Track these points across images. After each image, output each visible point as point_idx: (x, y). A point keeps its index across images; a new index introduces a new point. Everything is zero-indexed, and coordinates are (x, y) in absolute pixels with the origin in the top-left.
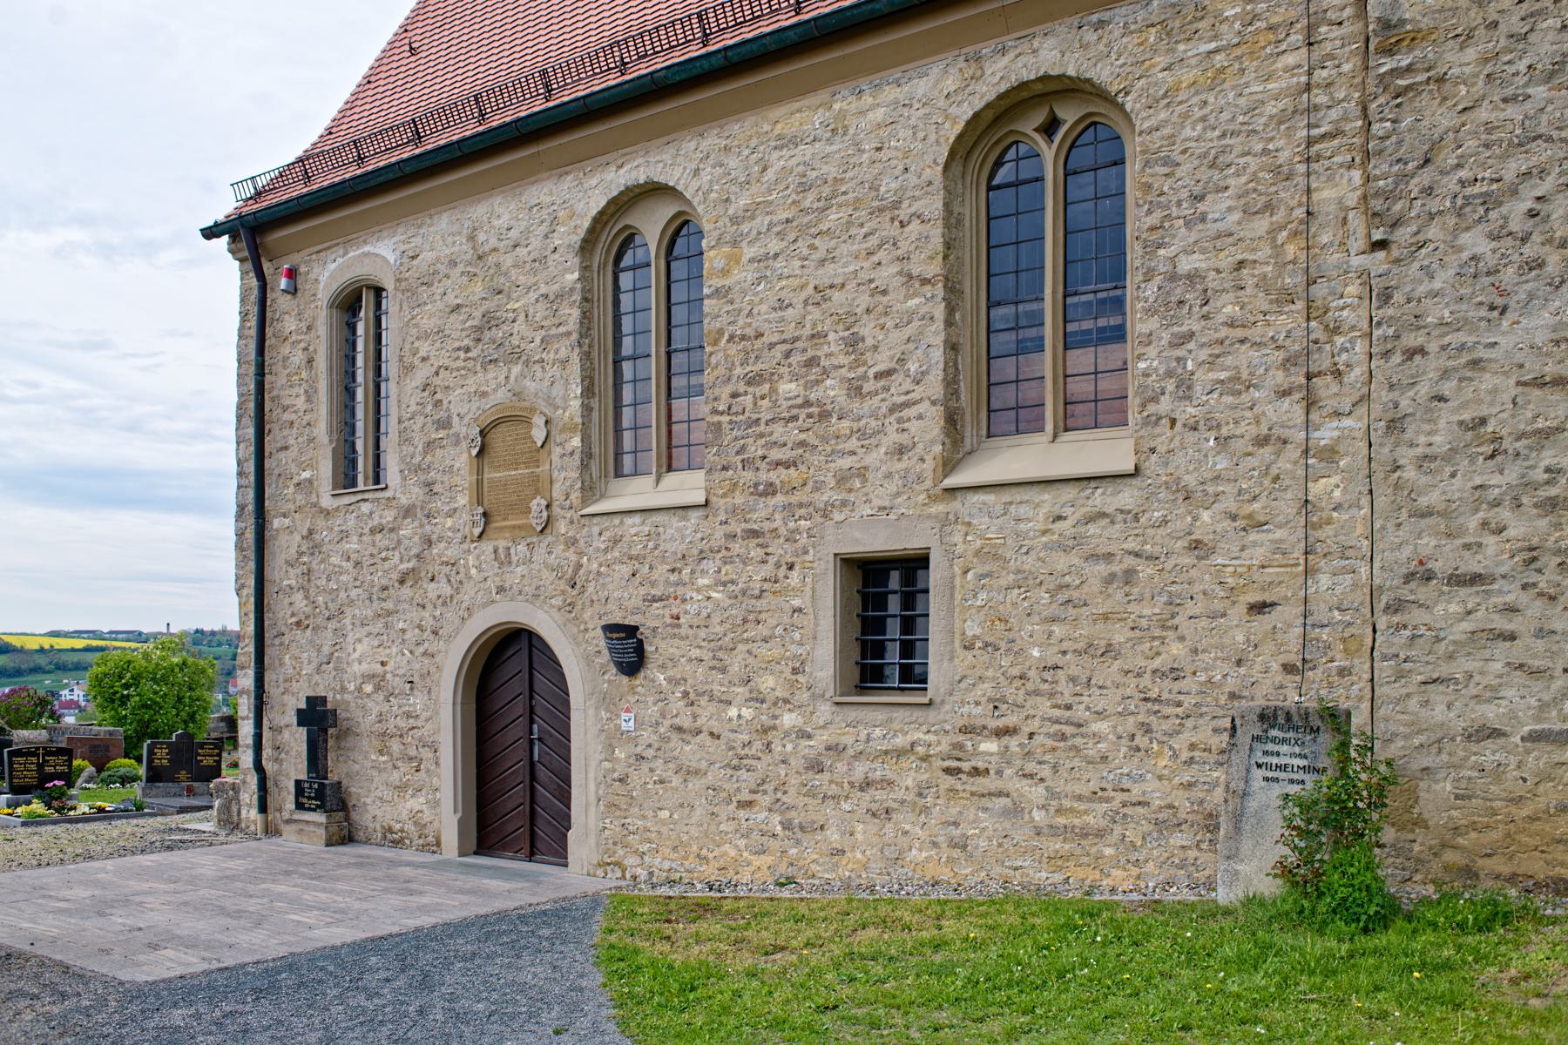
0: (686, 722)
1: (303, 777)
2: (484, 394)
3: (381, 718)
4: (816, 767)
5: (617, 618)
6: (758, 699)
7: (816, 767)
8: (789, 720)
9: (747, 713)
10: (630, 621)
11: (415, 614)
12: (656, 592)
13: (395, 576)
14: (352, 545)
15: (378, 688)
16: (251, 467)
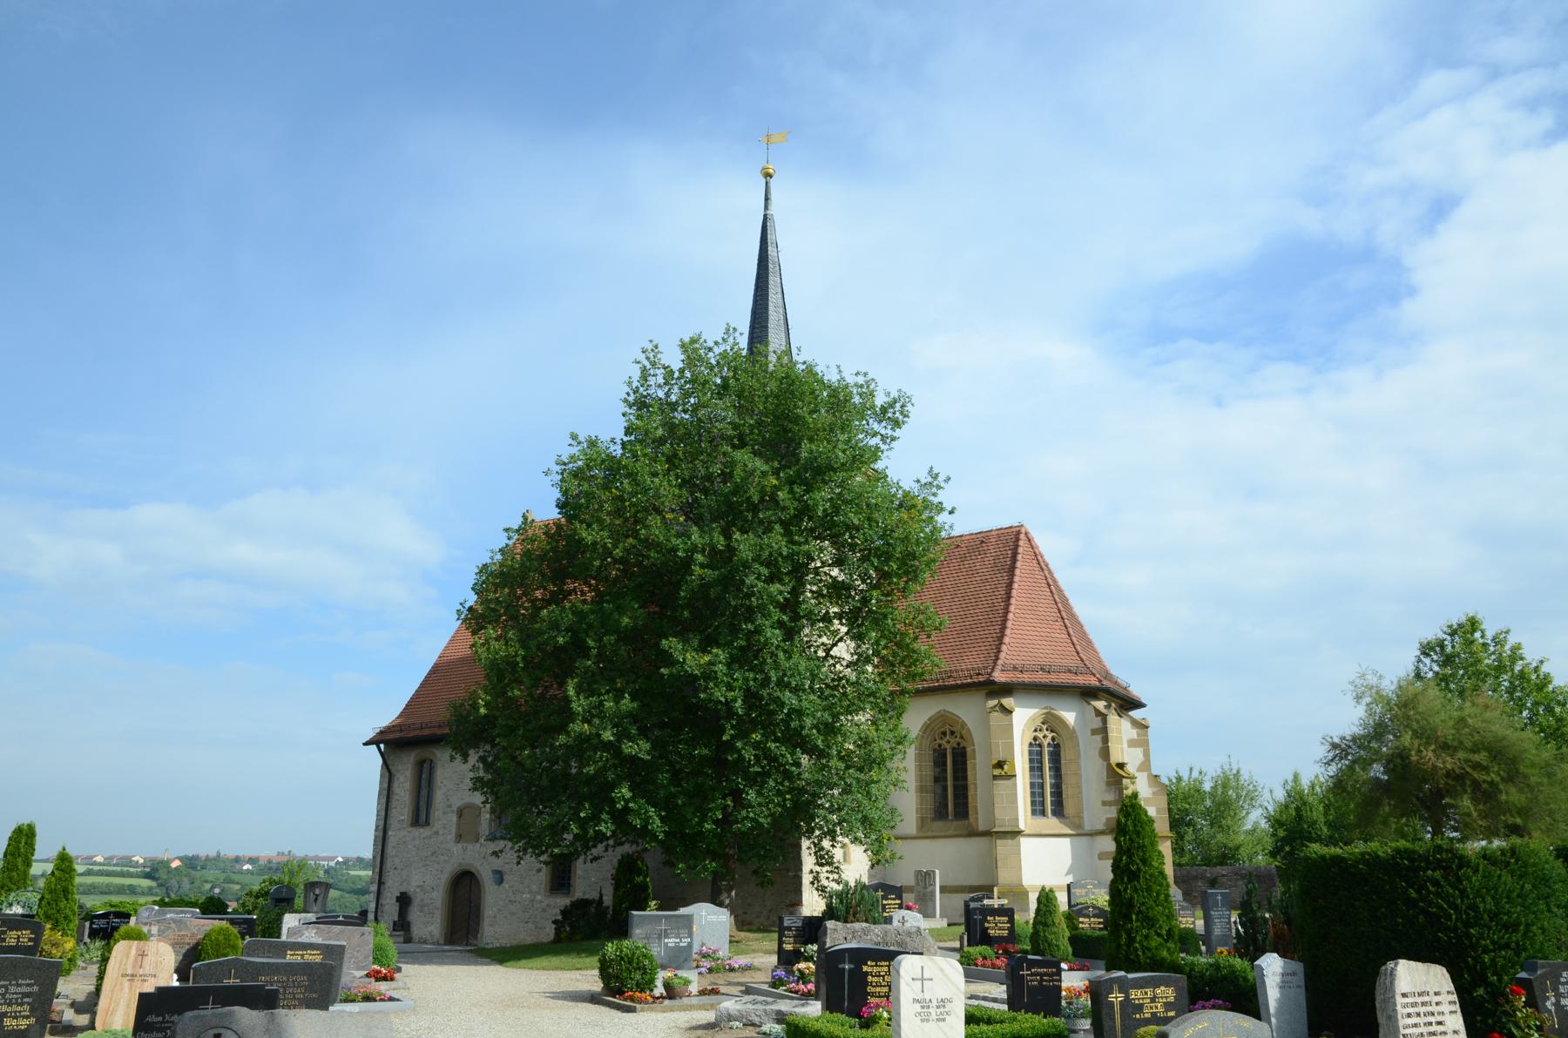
0: (512, 899)
1: (396, 919)
2: (463, 799)
3: (422, 900)
4: (544, 911)
5: (496, 869)
6: (531, 892)
7: (544, 911)
8: (539, 897)
9: (528, 896)
10: (500, 869)
11: (436, 866)
12: (507, 861)
13: (430, 853)
14: (417, 842)
15: (422, 890)
16: (383, 813)
